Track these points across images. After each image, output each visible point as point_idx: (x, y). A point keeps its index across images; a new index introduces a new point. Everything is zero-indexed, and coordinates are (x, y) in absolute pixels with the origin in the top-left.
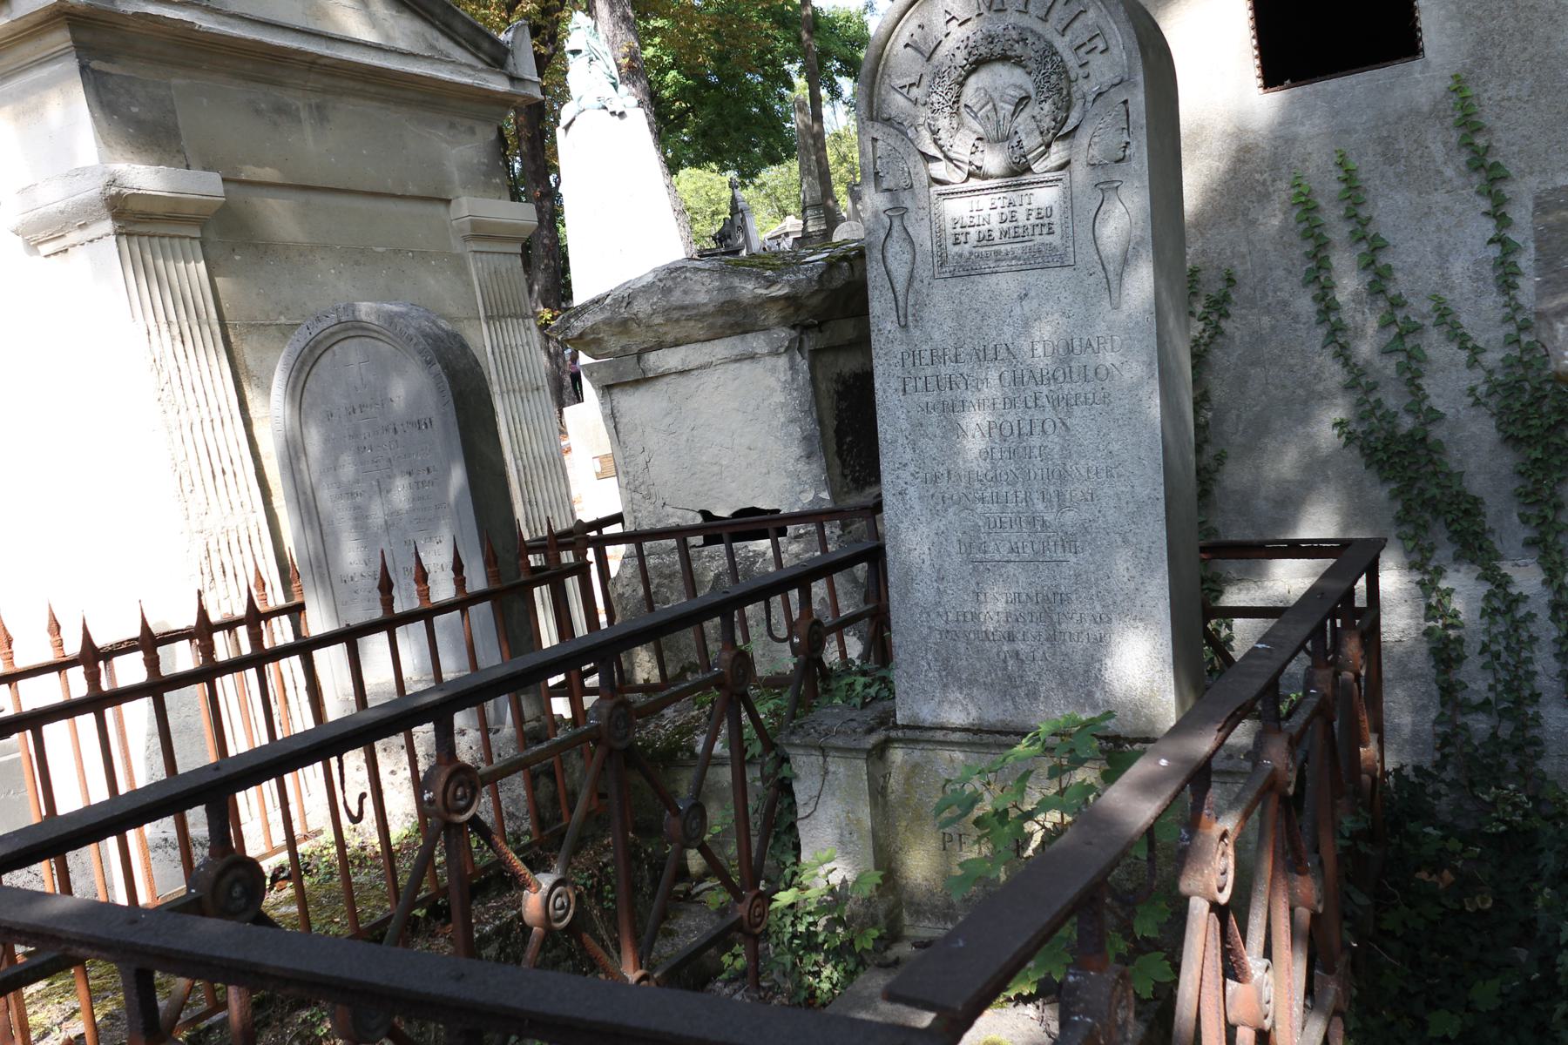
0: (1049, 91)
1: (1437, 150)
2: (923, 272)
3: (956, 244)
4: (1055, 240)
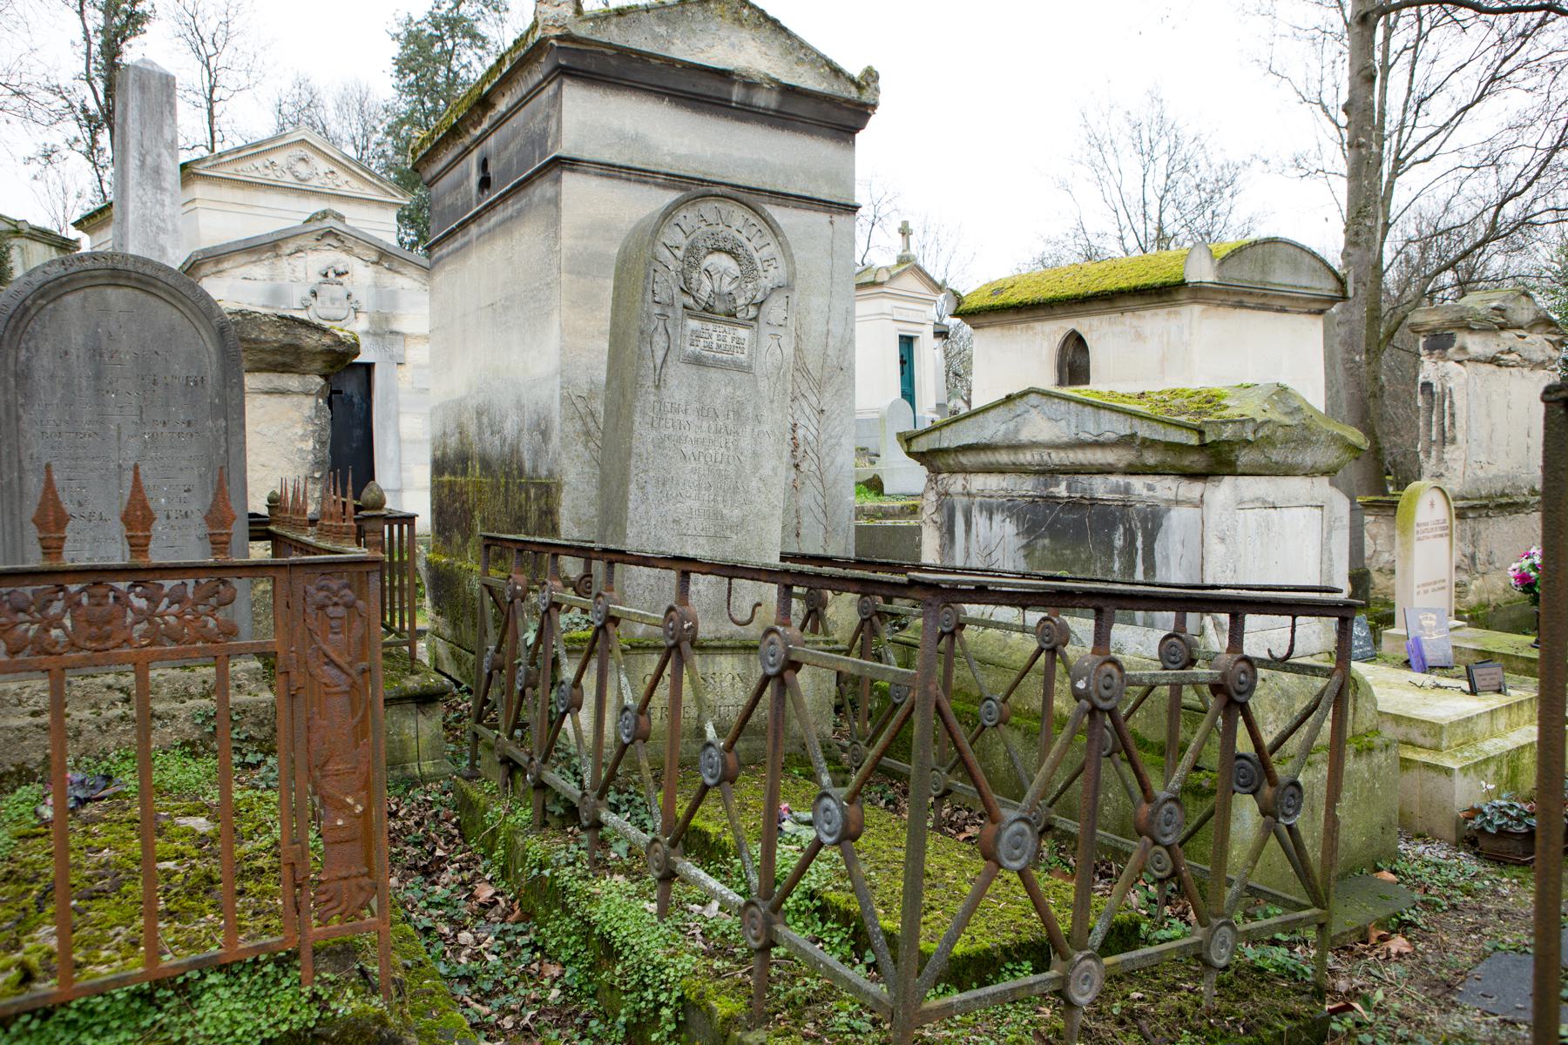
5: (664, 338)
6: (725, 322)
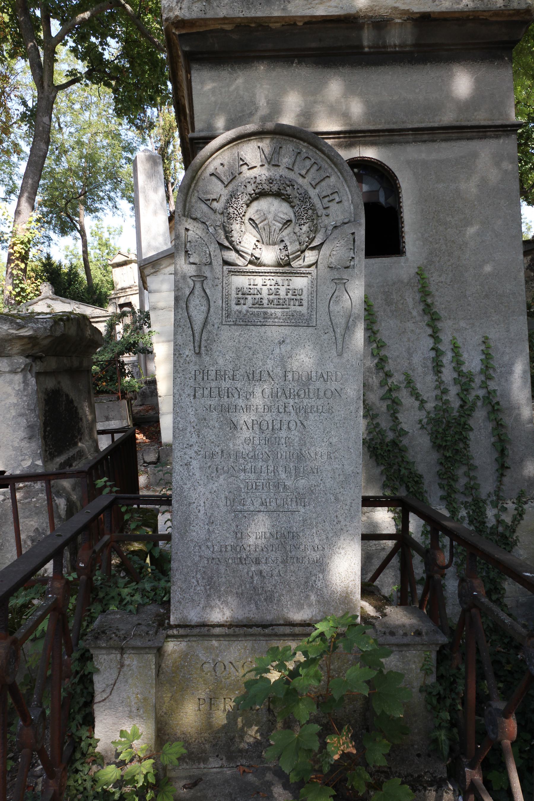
0: (307, 219)
1: (410, 302)
2: (214, 319)
3: (238, 304)
4: (303, 309)
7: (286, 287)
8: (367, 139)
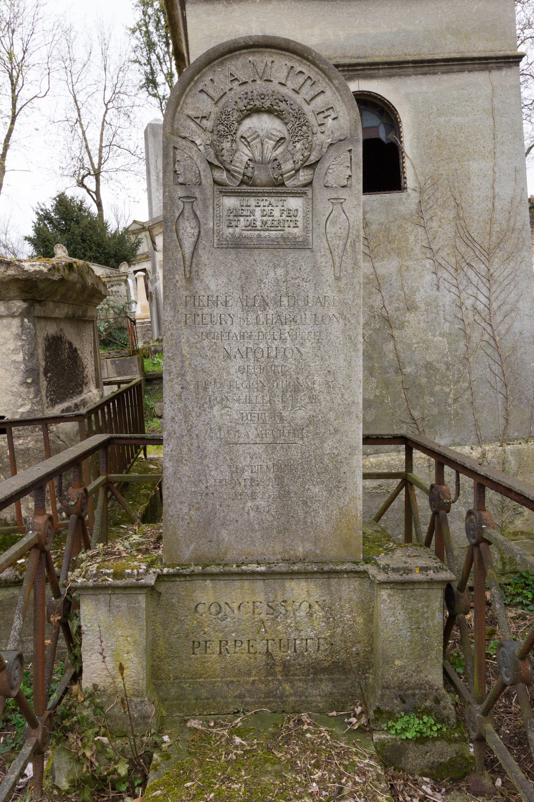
5: (194, 223)
6: (269, 194)
7: (280, 207)
8: (366, 72)
